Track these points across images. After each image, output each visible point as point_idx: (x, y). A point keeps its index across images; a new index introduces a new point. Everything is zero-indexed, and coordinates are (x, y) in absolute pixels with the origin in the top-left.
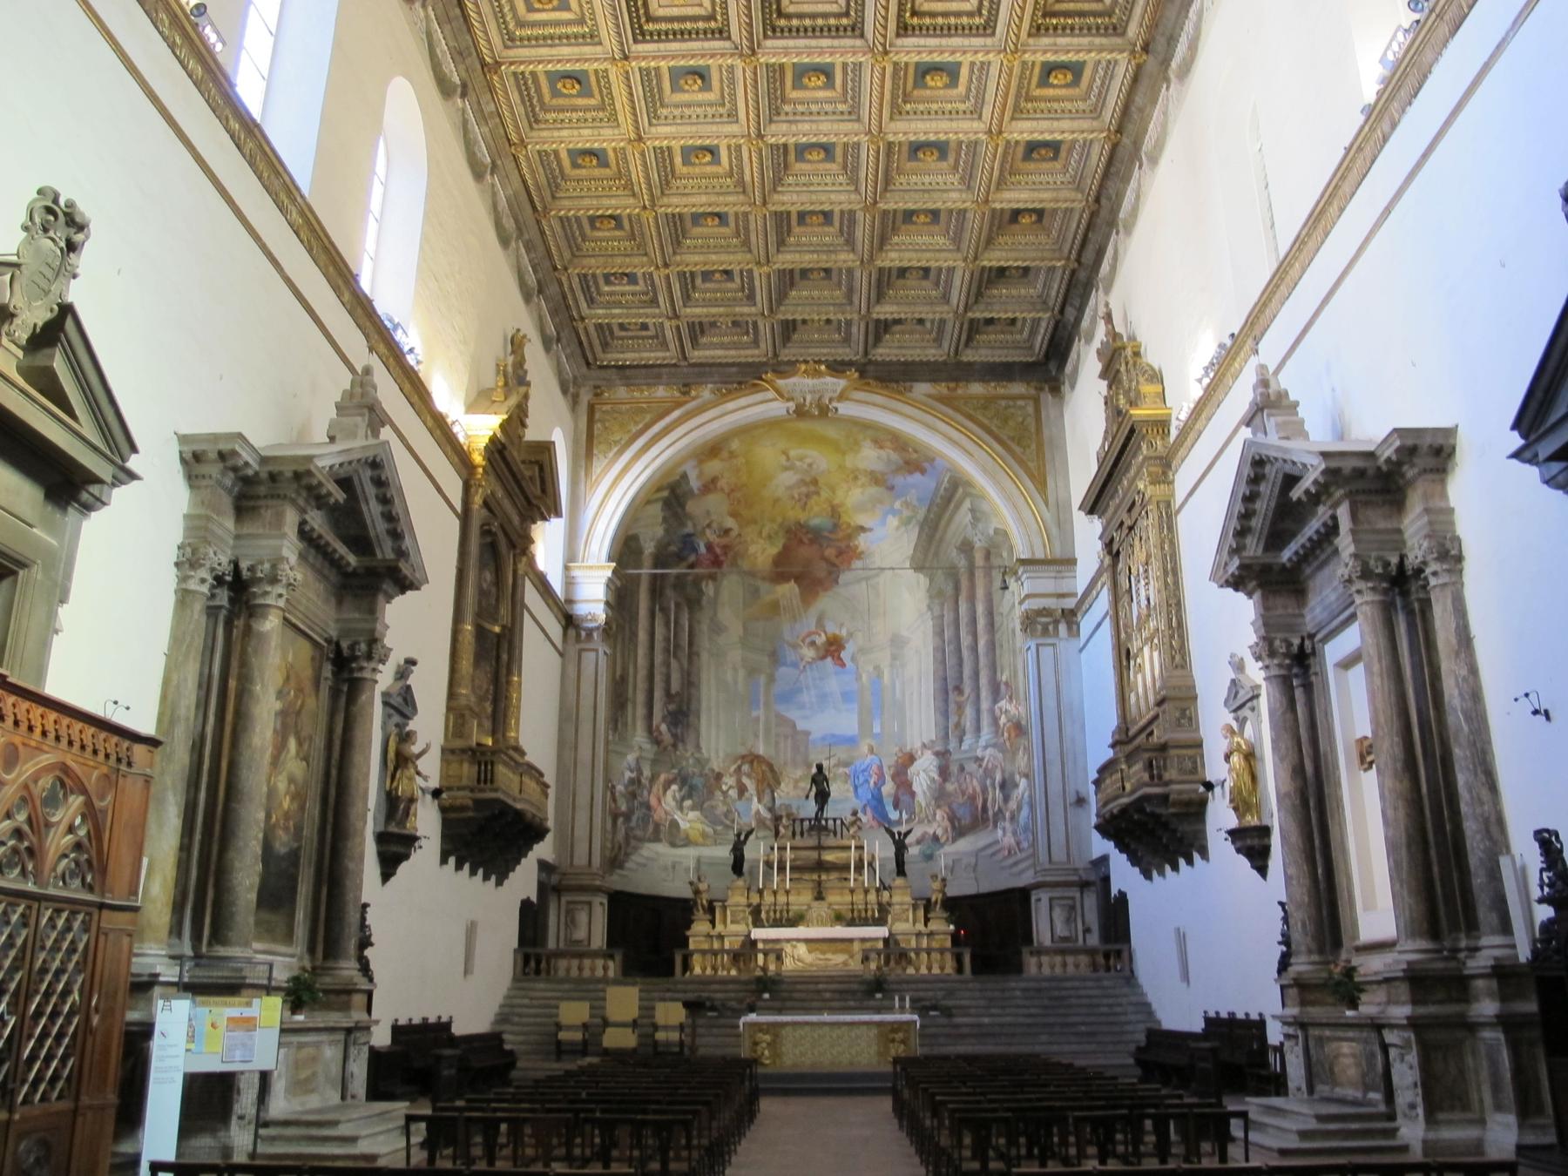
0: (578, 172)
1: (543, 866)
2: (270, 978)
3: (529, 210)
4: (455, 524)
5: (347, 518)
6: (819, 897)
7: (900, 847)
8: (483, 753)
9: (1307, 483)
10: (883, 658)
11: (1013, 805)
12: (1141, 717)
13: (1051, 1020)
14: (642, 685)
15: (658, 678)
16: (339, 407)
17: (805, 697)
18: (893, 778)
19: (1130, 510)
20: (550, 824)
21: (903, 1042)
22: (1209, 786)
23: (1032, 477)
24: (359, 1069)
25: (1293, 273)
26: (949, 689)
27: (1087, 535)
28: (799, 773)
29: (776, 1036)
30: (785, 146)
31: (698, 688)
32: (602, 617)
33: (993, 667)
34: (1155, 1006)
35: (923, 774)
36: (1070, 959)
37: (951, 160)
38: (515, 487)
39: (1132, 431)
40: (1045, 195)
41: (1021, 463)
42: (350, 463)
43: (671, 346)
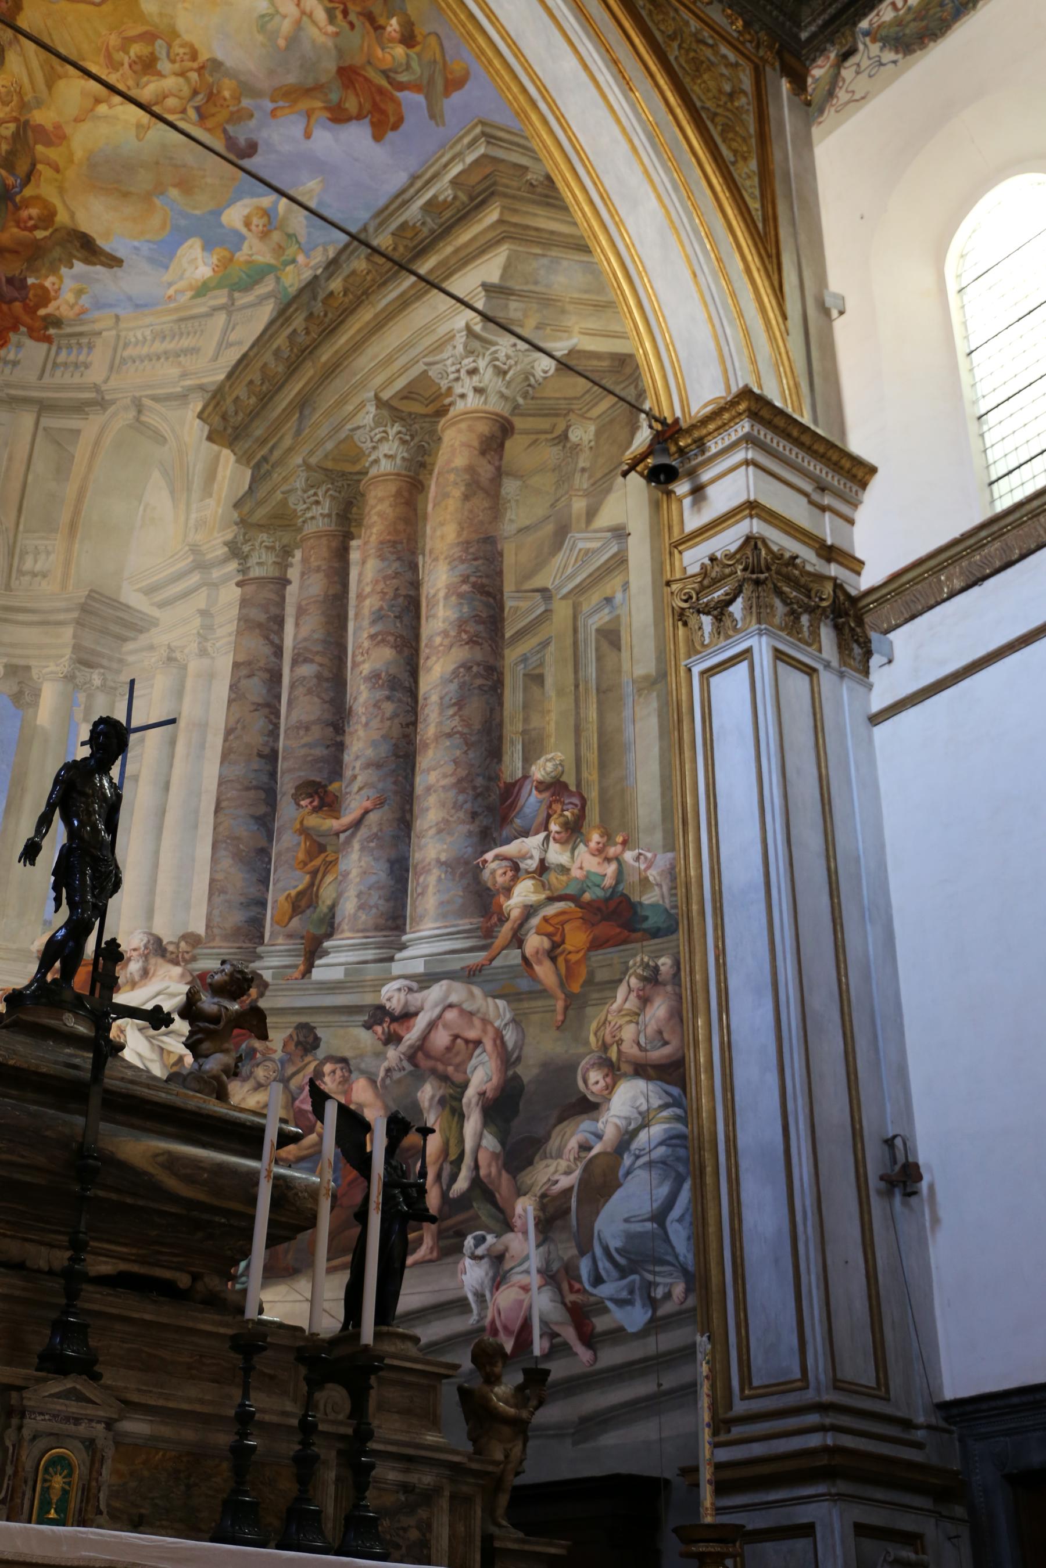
33: (487, 740)
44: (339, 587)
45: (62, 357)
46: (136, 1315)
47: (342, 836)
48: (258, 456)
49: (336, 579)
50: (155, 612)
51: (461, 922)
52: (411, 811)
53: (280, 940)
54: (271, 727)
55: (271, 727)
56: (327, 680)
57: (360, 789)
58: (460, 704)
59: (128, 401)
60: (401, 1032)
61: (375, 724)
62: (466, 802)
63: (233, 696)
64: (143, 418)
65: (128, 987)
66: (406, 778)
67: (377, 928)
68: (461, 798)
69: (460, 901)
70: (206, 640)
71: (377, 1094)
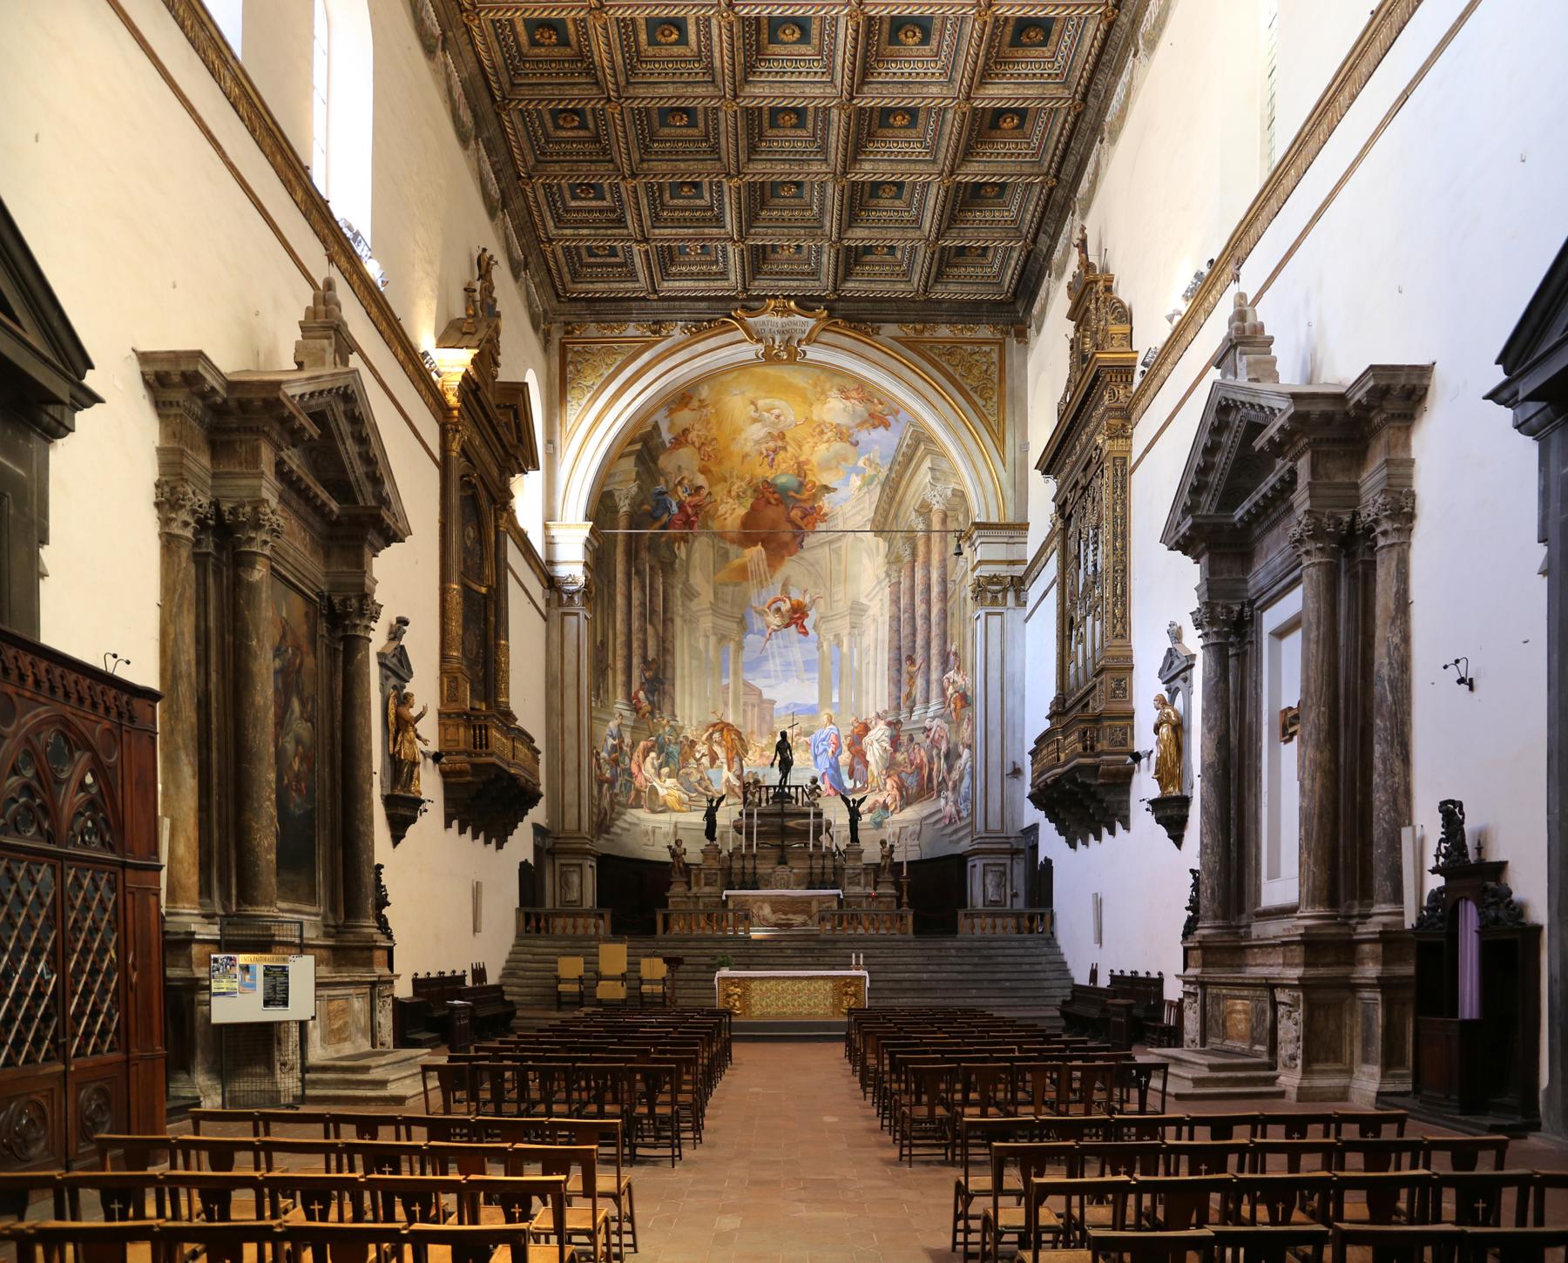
0: (536, 51)
1: (537, 828)
2: (301, 936)
3: (487, 101)
4: (434, 473)
5: (323, 455)
6: (782, 861)
7: (855, 815)
8: (477, 718)
9: (1272, 431)
10: (843, 625)
11: (955, 775)
12: (1079, 688)
13: (981, 976)
14: (620, 652)
15: (635, 645)
16: (303, 327)
17: (770, 666)
18: (849, 747)
19: (1085, 469)
20: (543, 789)
21: (854, 995)
22: (1137, 757)
23: (991, 431)
24: (385, 1019)
25: (1287, 182)
26: (902, 659)
27: (1042, 493)
28: (765, 741)
29: (746, 989)
30: (757, 19)
31: (673, 655)
32: (582, 580)
34: (1069, 965)
35: (876, 745)
36: (999, 921)
37: (934, 43)
38: (489, 438)
39: (1096, 378)
40: (1031, 92)
41: (983, 417)
42: (321, 393)
43: (641, 276)
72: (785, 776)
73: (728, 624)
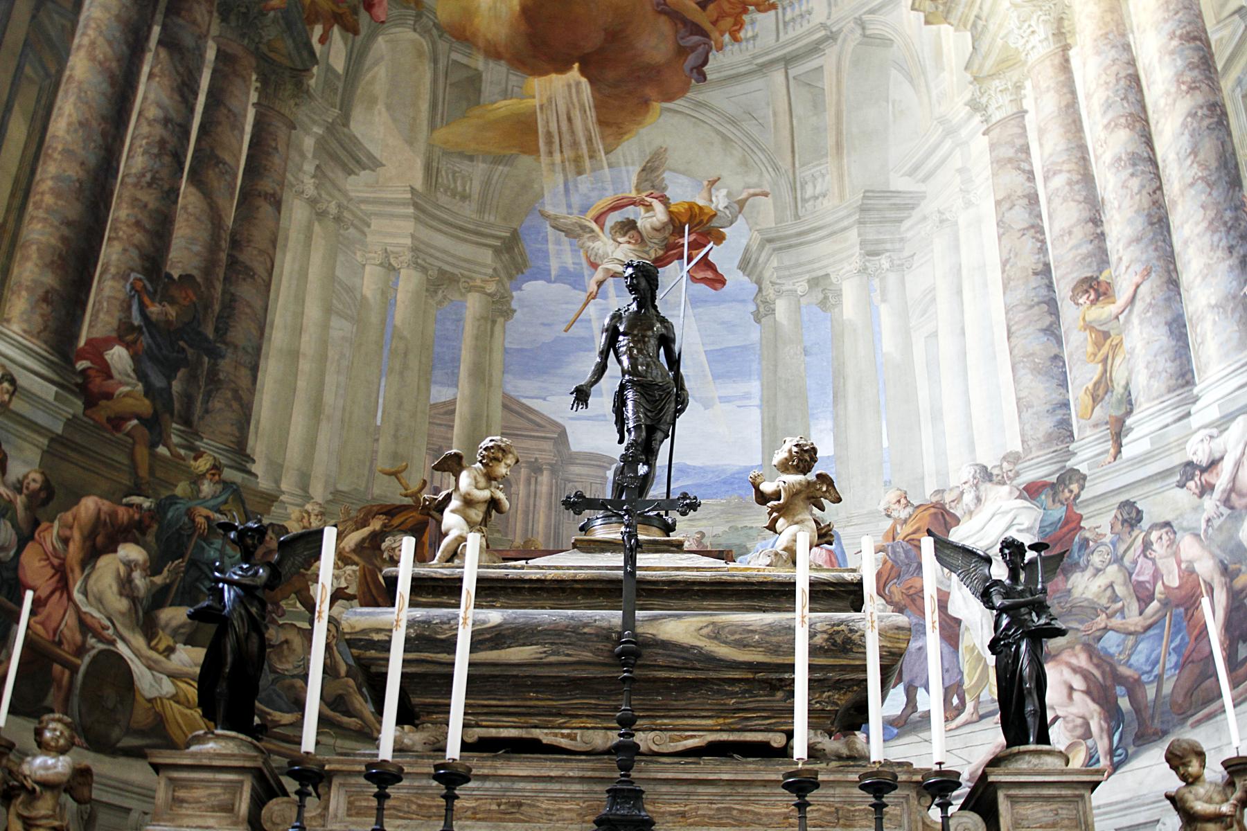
15: (120, 212)
44: (1069, 96)
45: (789, 15)
46: (711, 777)
47: (1121, 317)
48: (972, 18)
49: (1065, 90)
50: (922, 187)
51: (1240, 356)
52: (1176, 269)
53: (1088, 432)
54: (1039, 244)
55: (1039, 244)
56: (1077, 182)
57: (1127, 268)
58: (1194, 152)
59: (852, 24)
60: (1212, 481)
61: (1127, 202)
62: (1220, 240)
63: (1001, 231)
64: (868, 32)
65: (967, 517)
66: (1164, 241)
67: (1170, 390)
68: (1216, 238)
69: (1236, 335)
70: (968, 192)
71: (1203, 547)
72: (645, 449)
73: (464, 250)
